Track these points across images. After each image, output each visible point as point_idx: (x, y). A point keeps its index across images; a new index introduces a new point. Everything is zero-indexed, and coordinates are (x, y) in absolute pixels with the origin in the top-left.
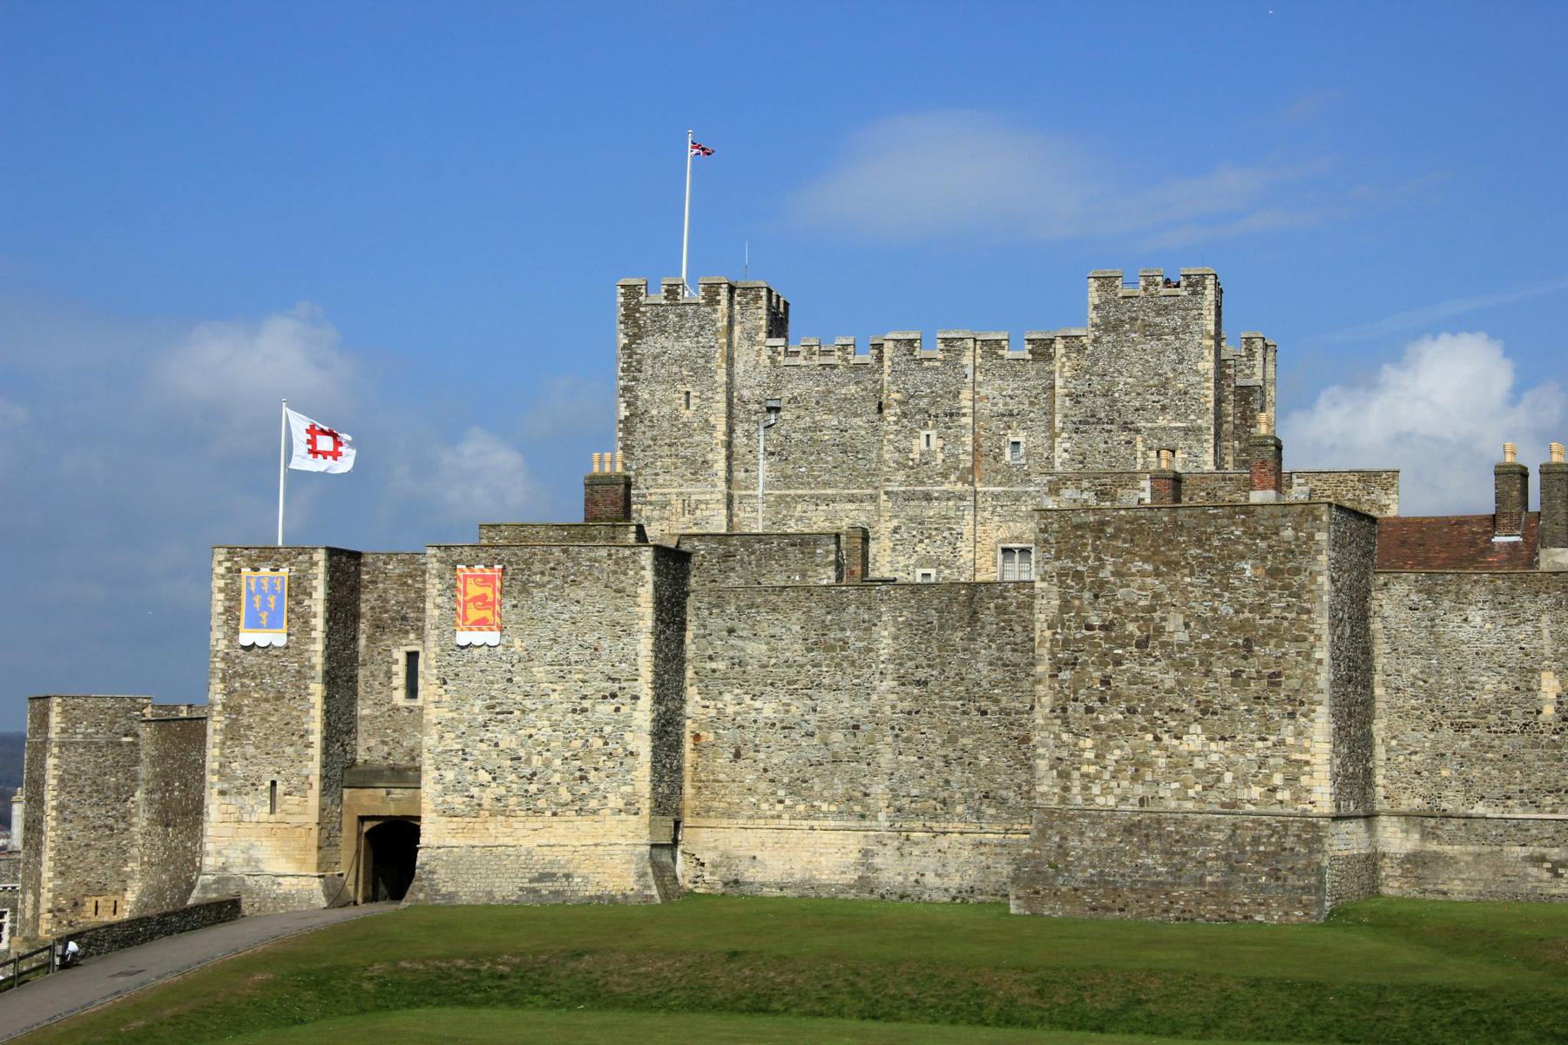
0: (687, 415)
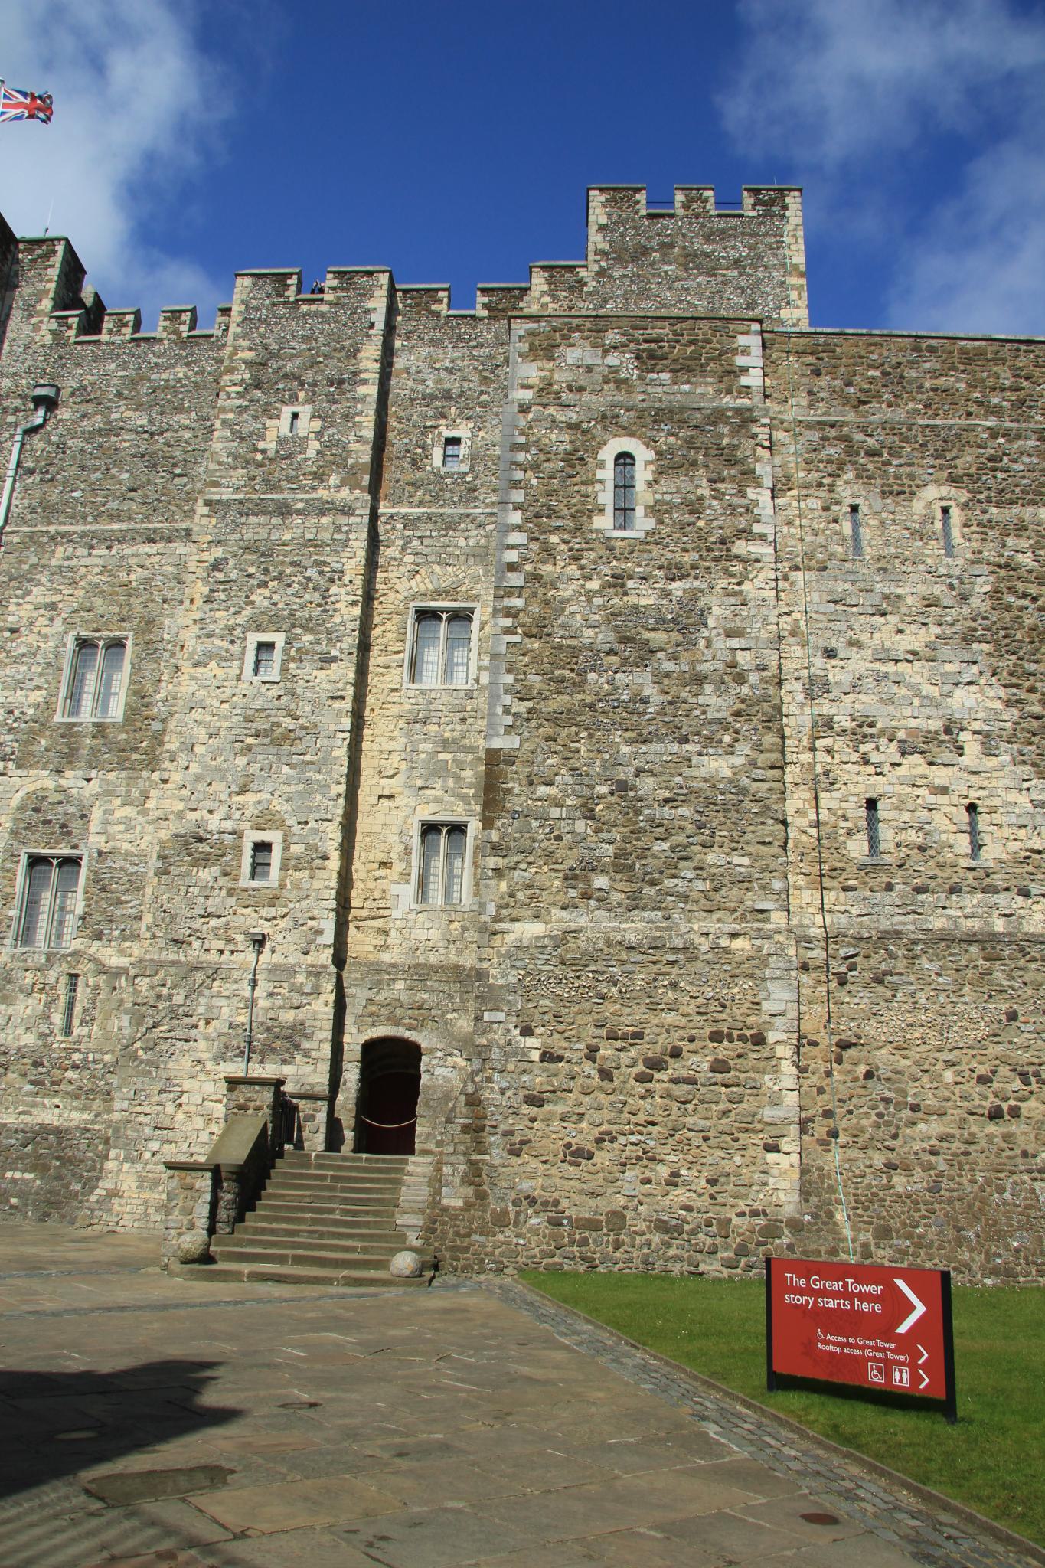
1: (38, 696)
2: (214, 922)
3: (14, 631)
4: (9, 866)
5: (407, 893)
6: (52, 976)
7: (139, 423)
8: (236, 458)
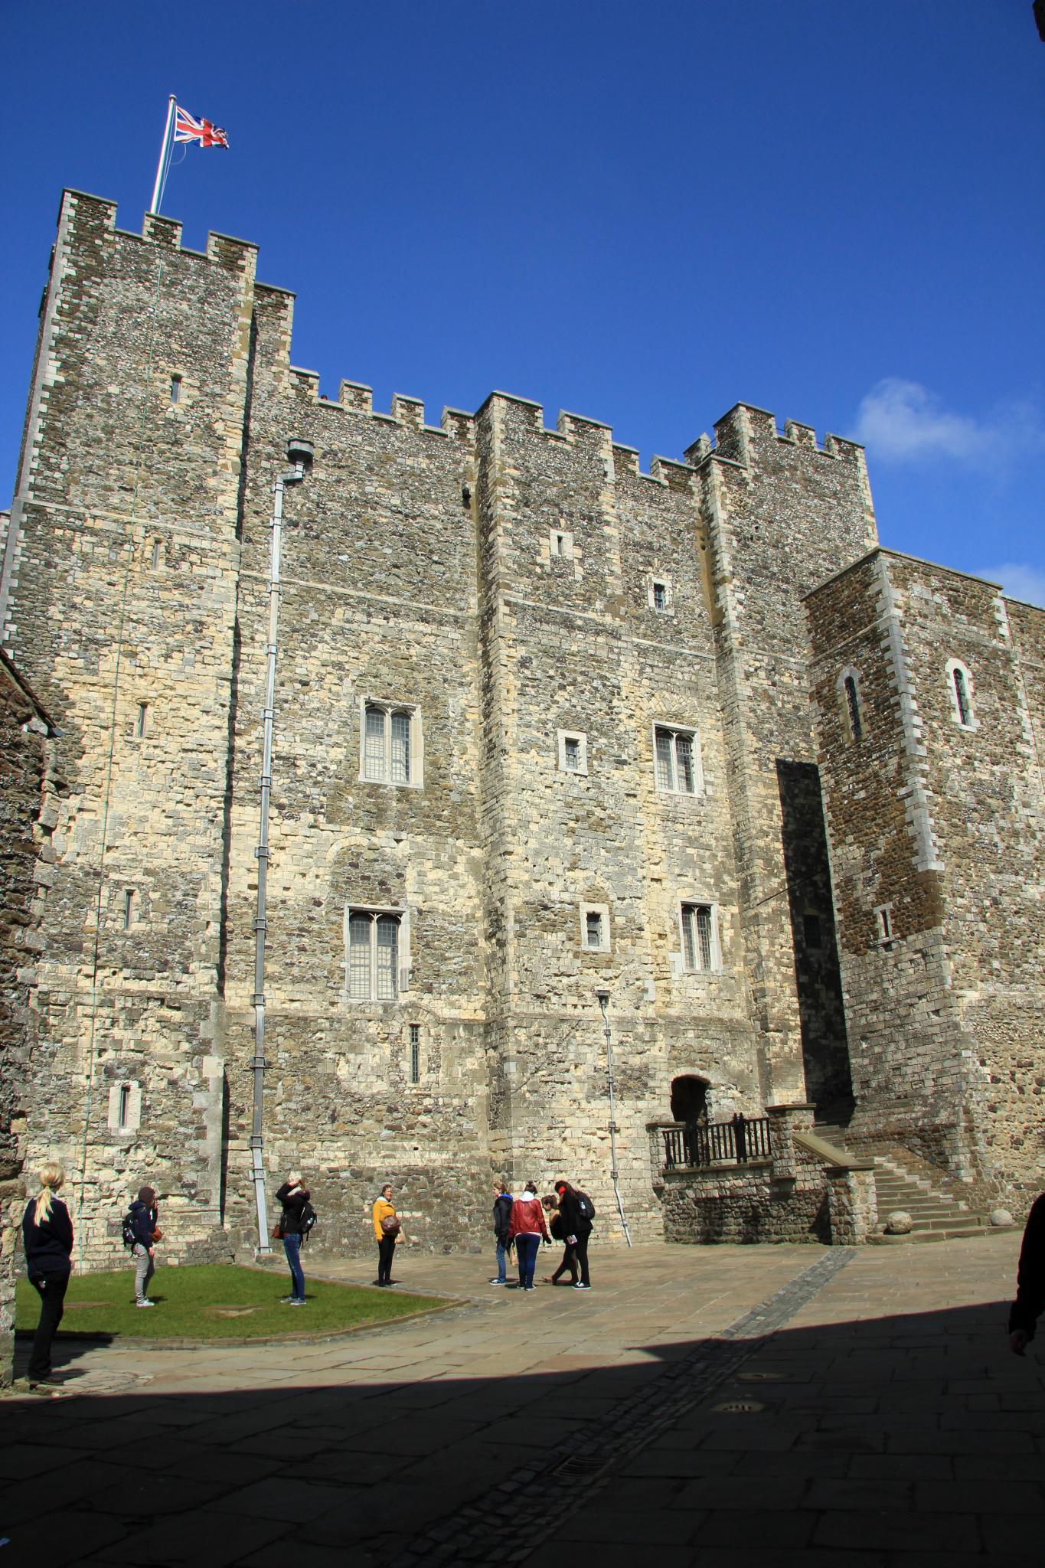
0: (175, 409)
1: (338, 753)
2: (565, 980)
3: (305, 684)
4: (334, 918)
5: (679, 959)
6: (395, 1026)
7: (393, 502)
8: (519, 565)
